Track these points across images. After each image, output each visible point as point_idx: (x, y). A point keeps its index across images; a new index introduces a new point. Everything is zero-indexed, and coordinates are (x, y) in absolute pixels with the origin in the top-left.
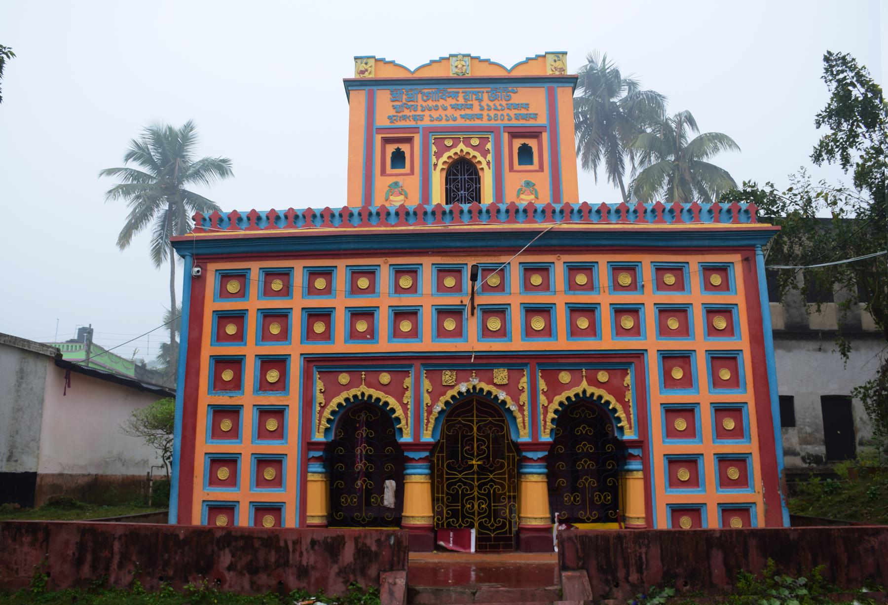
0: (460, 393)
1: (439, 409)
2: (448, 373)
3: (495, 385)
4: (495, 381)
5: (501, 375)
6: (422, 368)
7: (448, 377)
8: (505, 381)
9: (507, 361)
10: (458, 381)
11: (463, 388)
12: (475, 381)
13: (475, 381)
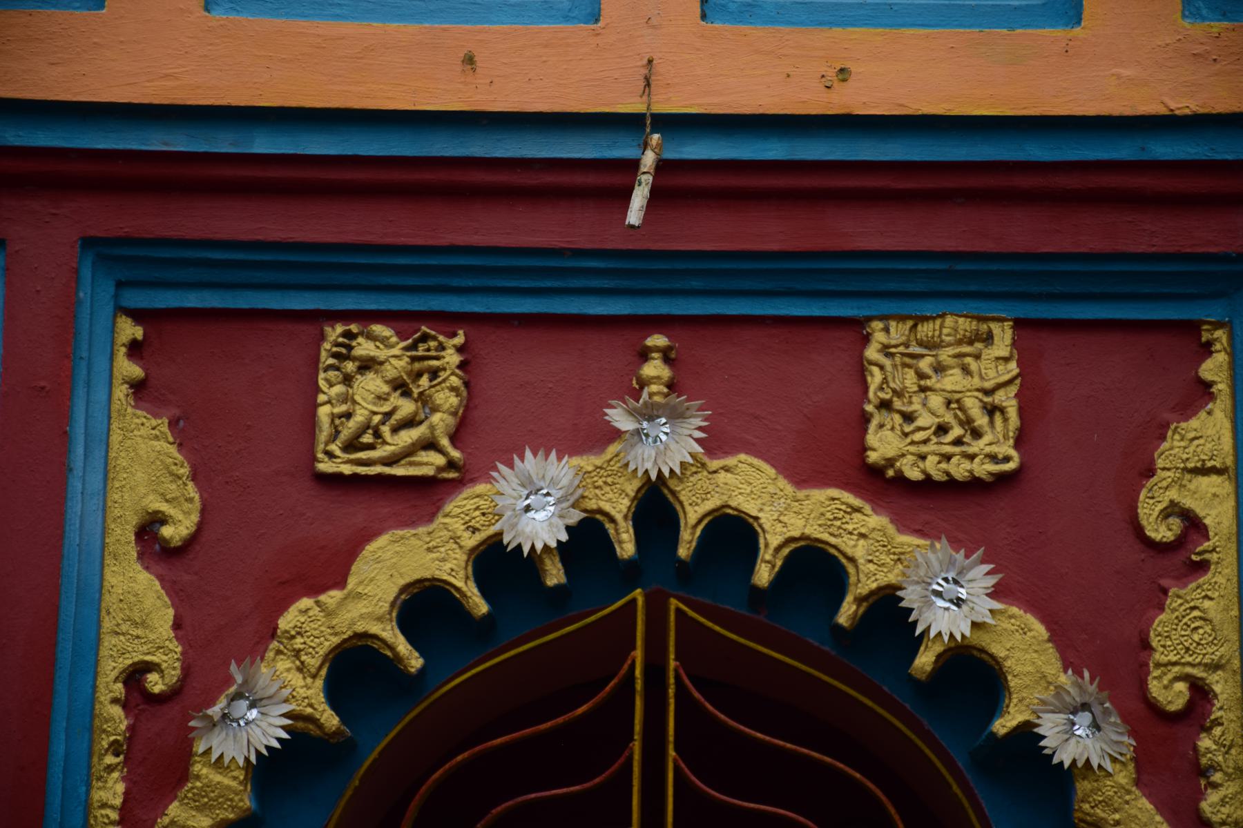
0: (497, 562)
1: (264, 729)
2: (385, 347)
3: (879, 484)
4: (883, 443)
5: (948, 387)
6: (94, 292)
7: (374, 391)
8: (995, 450)
9: (1018, 231)
10: (480, 444)
11: (534, 505)
12: (668, 446)
13: (668, 446)
